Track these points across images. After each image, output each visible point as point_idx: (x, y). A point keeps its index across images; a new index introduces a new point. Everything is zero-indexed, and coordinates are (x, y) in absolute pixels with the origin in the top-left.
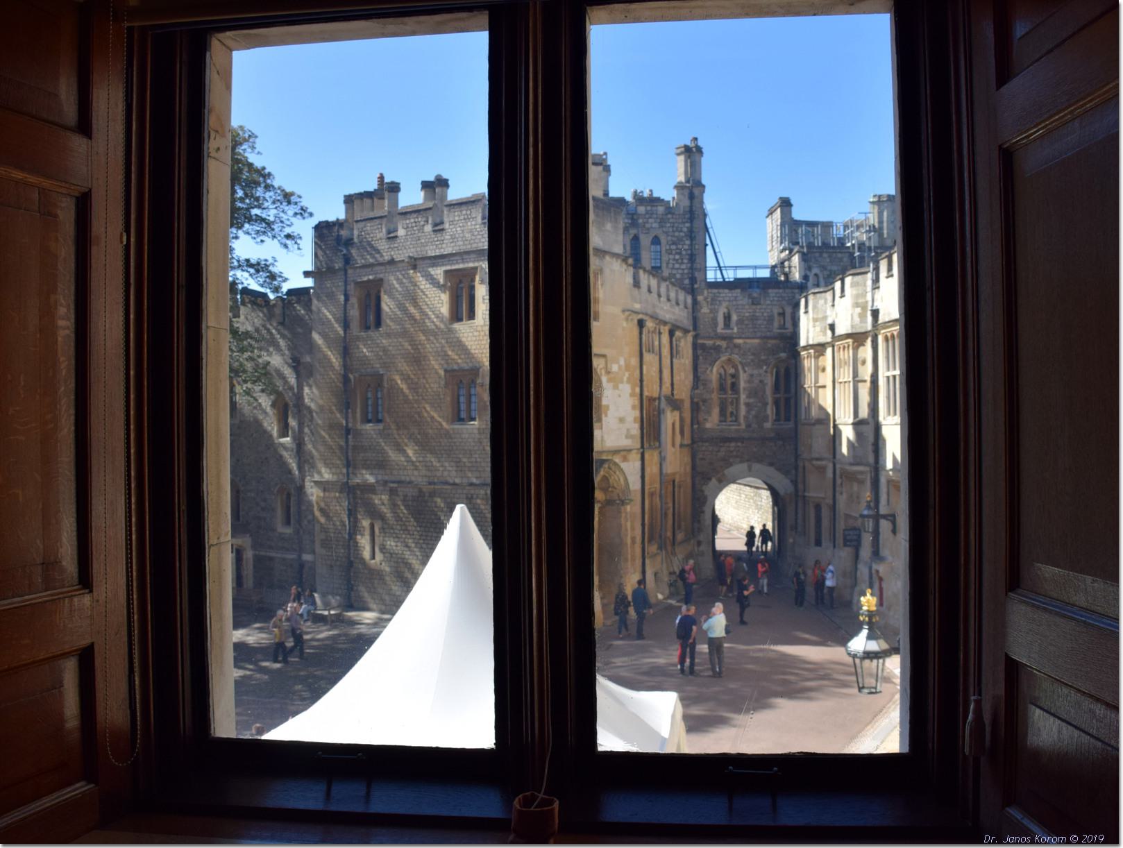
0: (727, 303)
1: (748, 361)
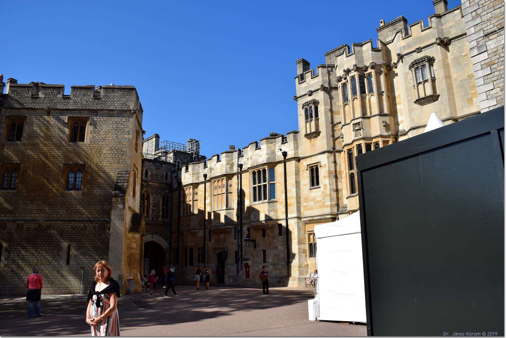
0: (147, 167)
1: (154, 192)
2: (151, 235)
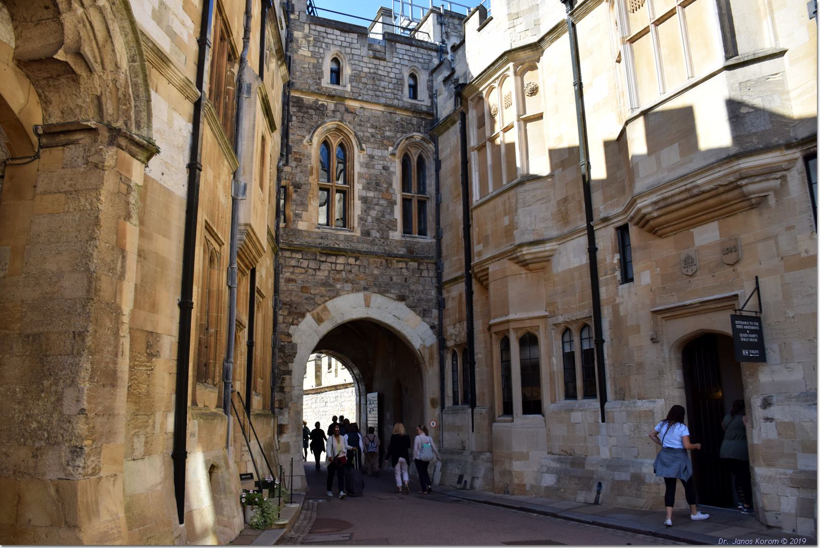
1: (367, 134)
2: (360, 296)
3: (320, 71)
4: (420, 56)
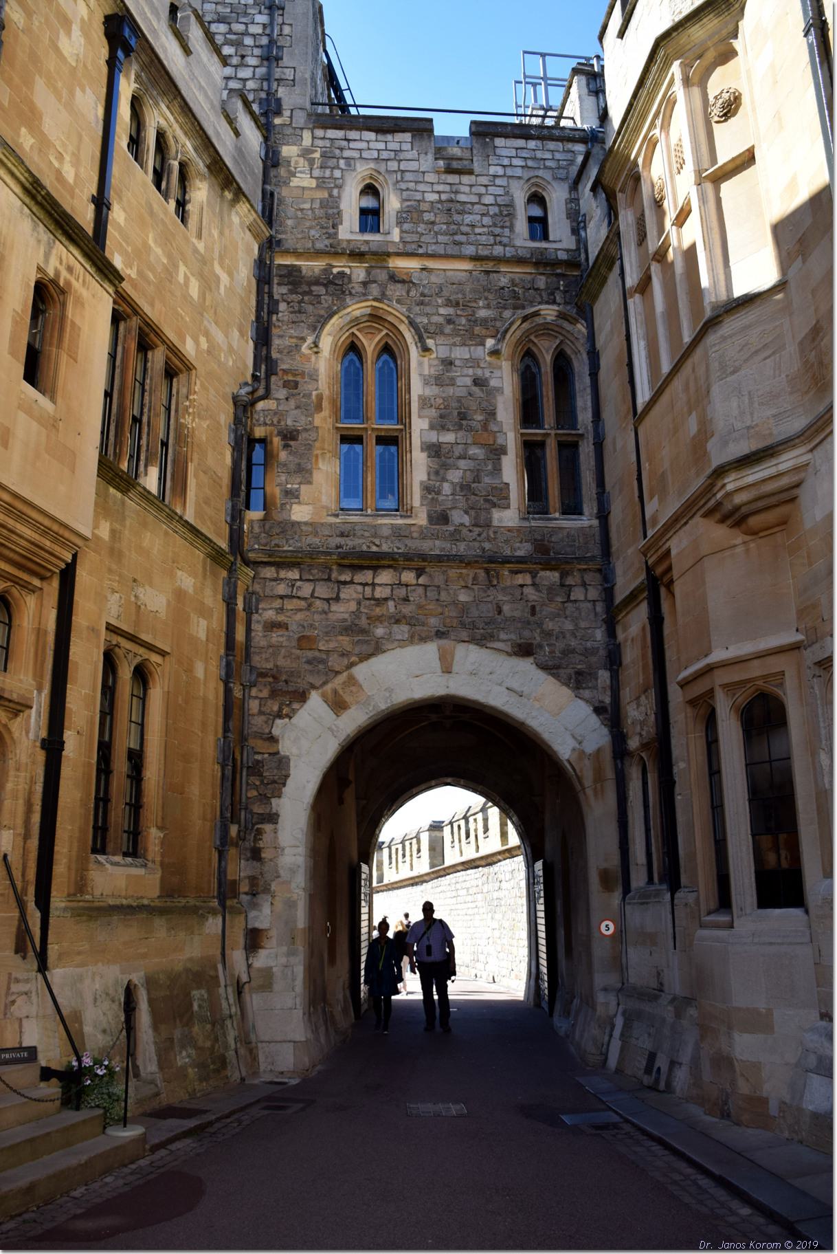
0: (372, 165)
1: (435, 319)
2: (431, 650)
3: (335, 211)
4: (548, 155)
